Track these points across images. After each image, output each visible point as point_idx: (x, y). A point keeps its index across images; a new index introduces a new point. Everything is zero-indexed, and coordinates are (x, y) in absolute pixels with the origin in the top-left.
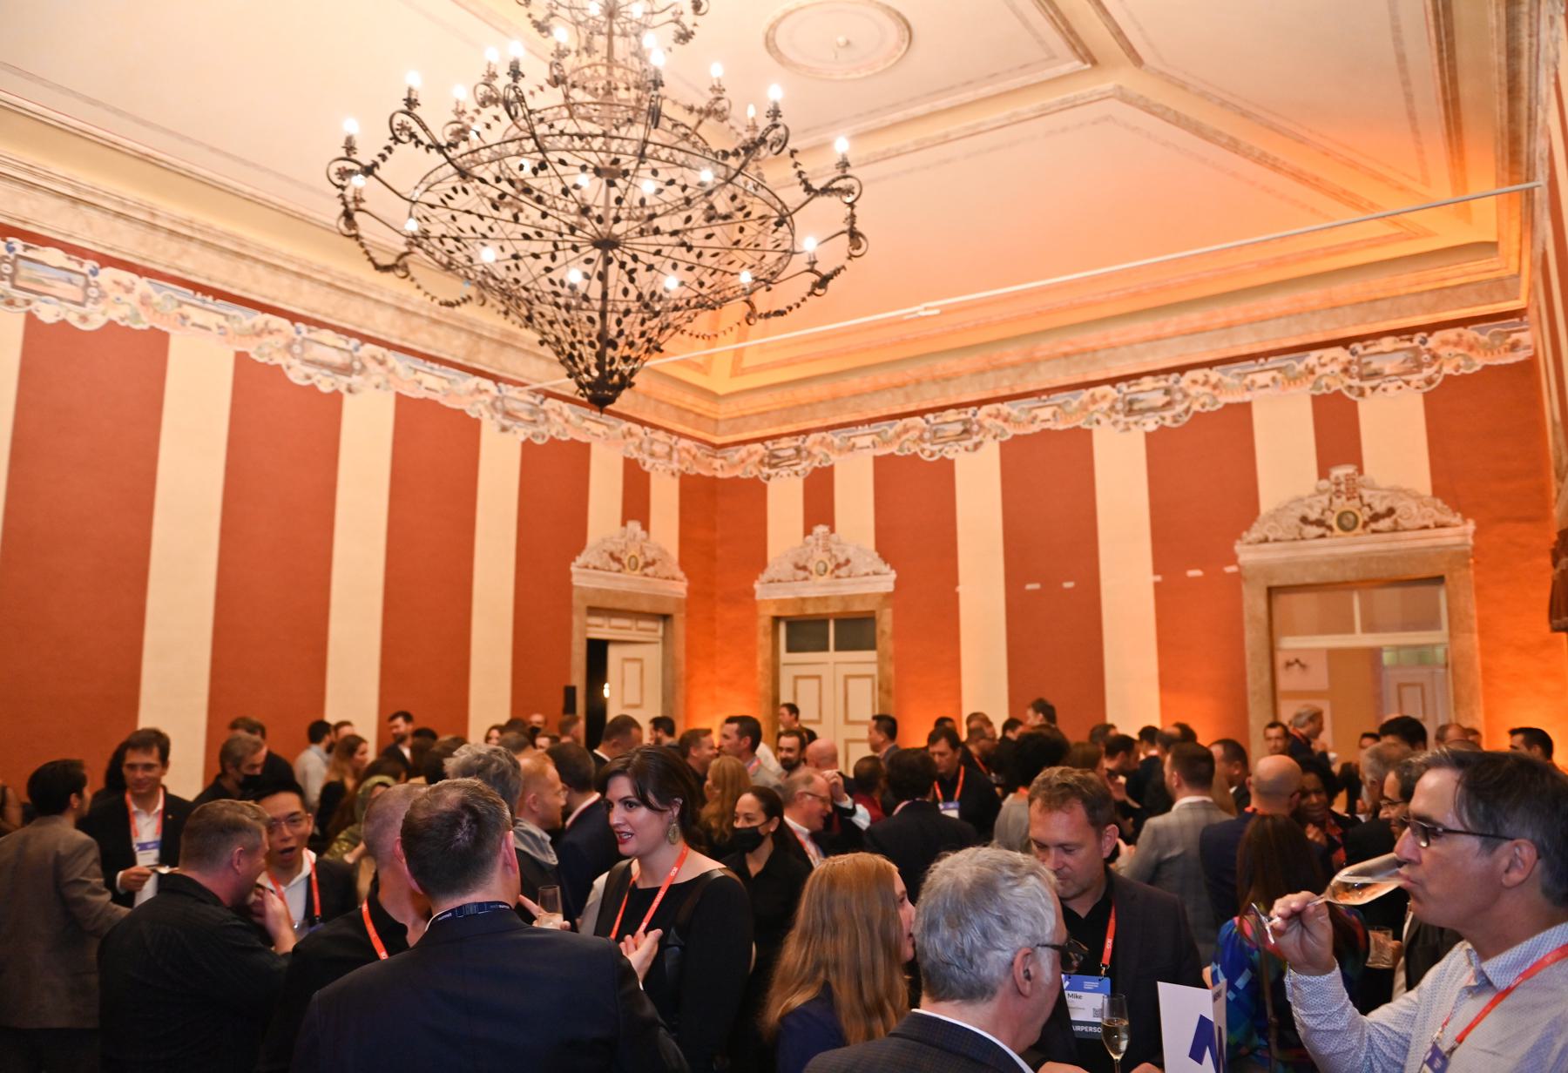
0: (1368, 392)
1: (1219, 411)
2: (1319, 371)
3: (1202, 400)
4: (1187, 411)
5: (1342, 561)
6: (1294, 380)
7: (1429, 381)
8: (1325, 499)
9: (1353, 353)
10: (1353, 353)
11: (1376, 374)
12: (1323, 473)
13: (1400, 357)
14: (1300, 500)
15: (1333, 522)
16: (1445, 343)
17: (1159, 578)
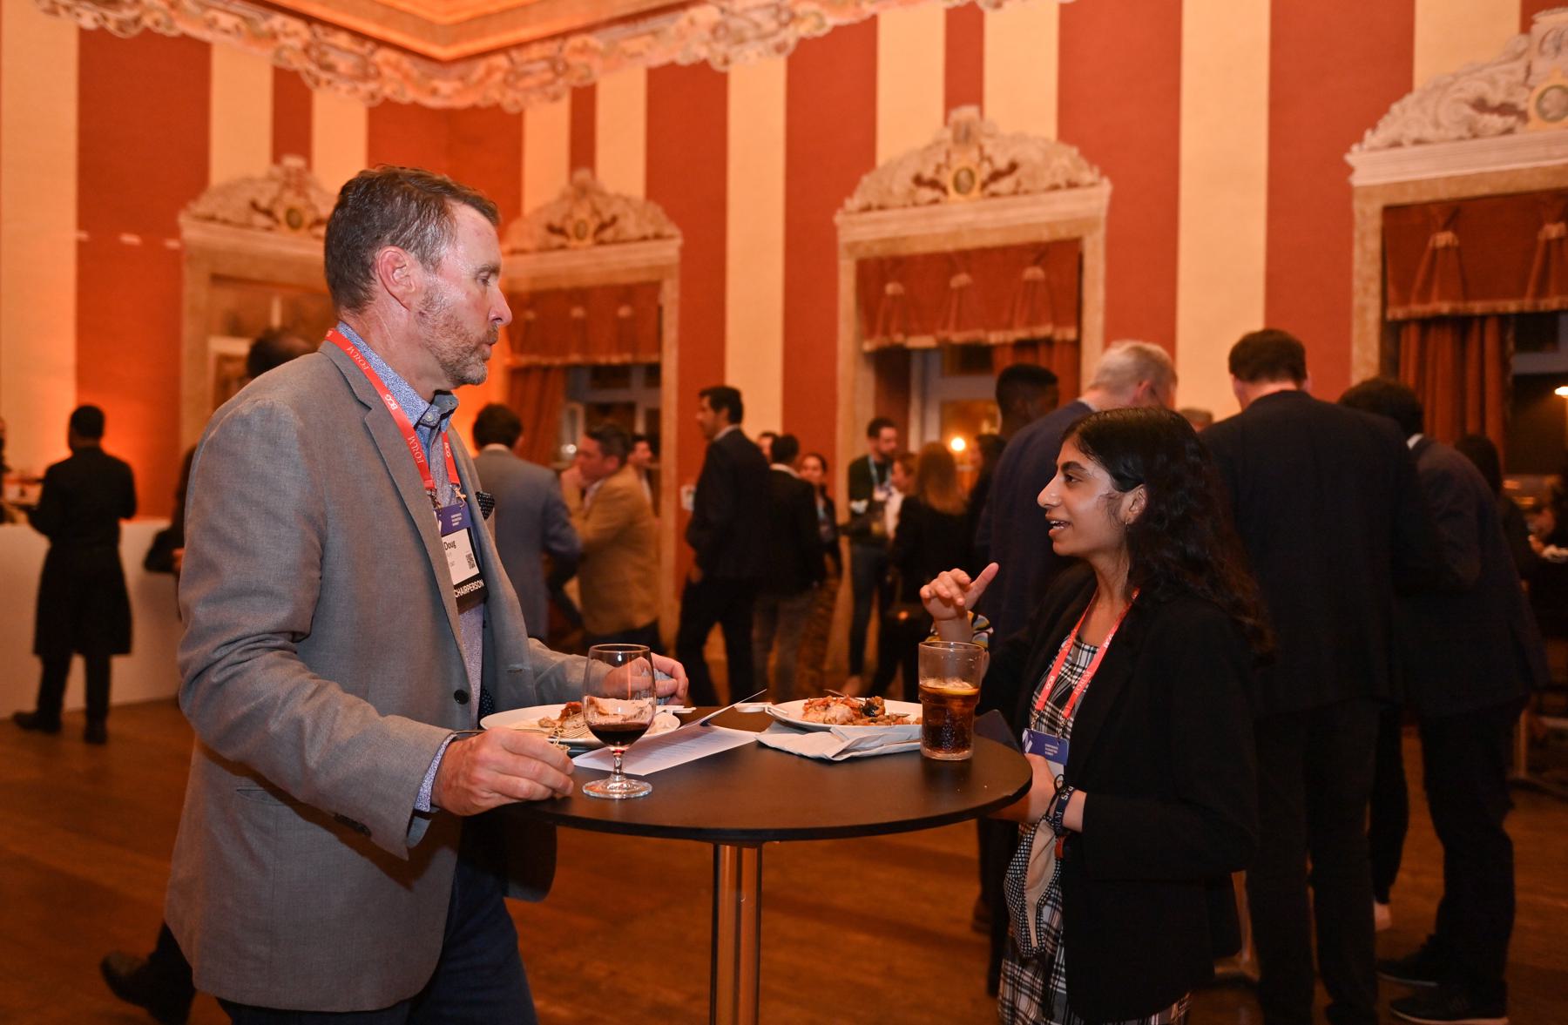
0: (323, 84)
1: (174, 39)
2: (283, 40)
3: (158, 15)
4: (137, 21)
5: (285, 262)
6: (258, 37)
7: (373, 96)
8: (274, 188)
9: (315, 35)
10: (315, 35)
11: (329, 68)
12: (276, 158)
13: (352, 60)
14: (250, 180)
15: (281, 214)
16: (388, 63)
17: (84, 236)
